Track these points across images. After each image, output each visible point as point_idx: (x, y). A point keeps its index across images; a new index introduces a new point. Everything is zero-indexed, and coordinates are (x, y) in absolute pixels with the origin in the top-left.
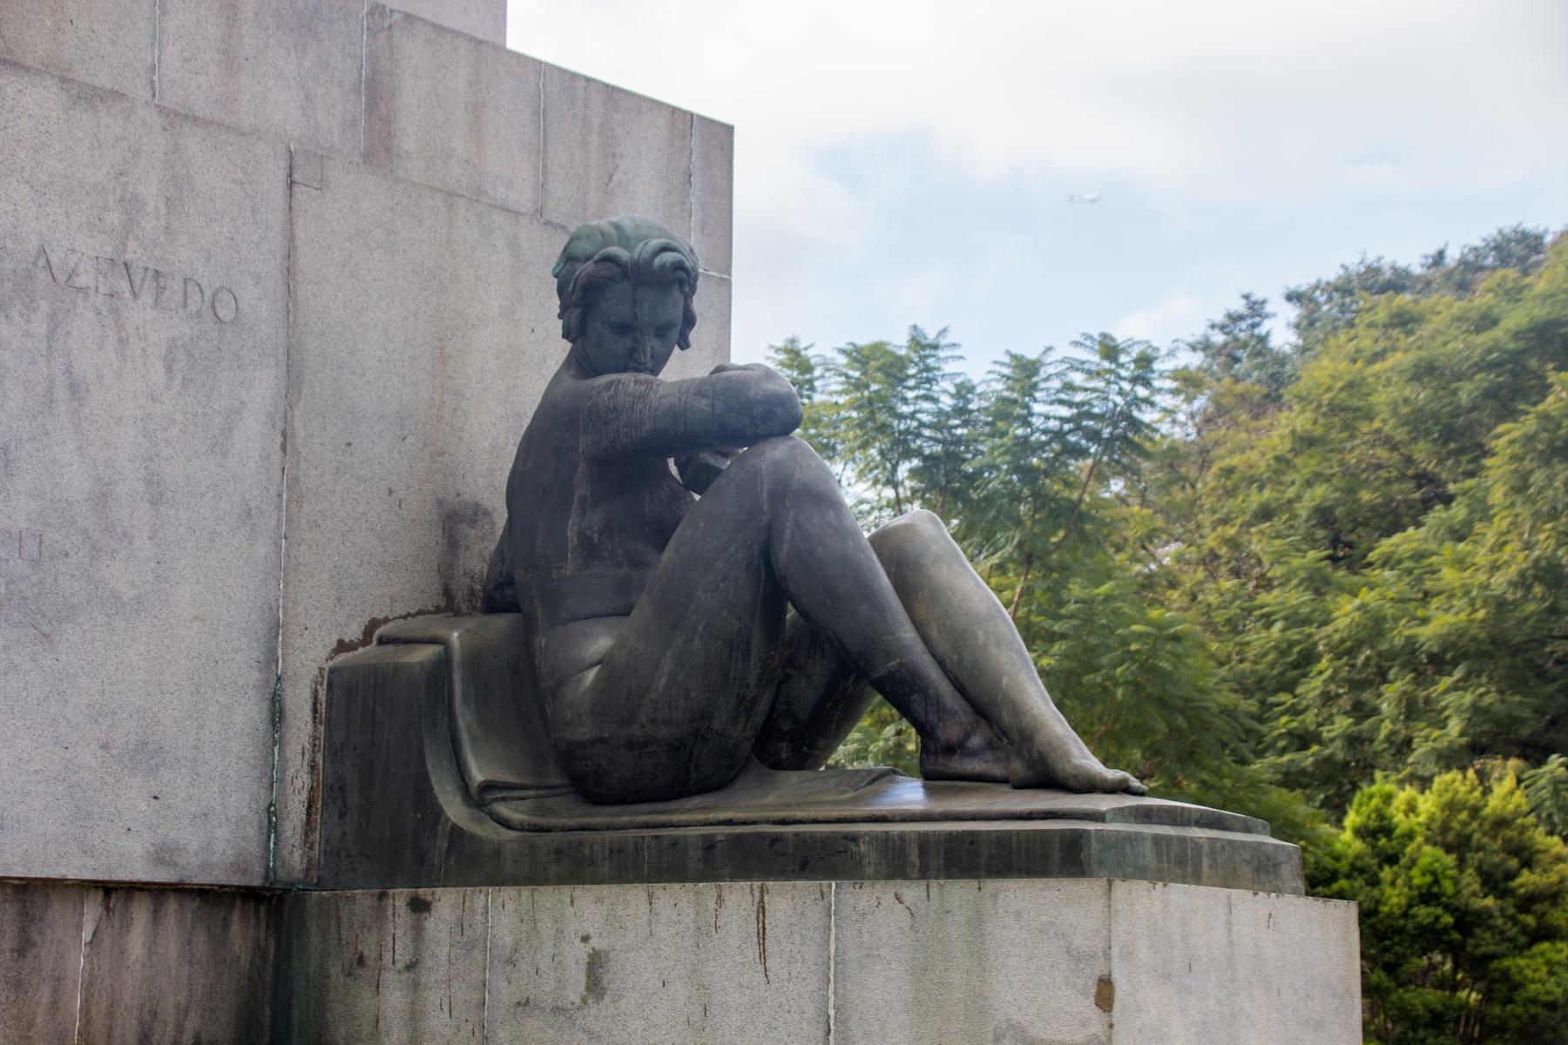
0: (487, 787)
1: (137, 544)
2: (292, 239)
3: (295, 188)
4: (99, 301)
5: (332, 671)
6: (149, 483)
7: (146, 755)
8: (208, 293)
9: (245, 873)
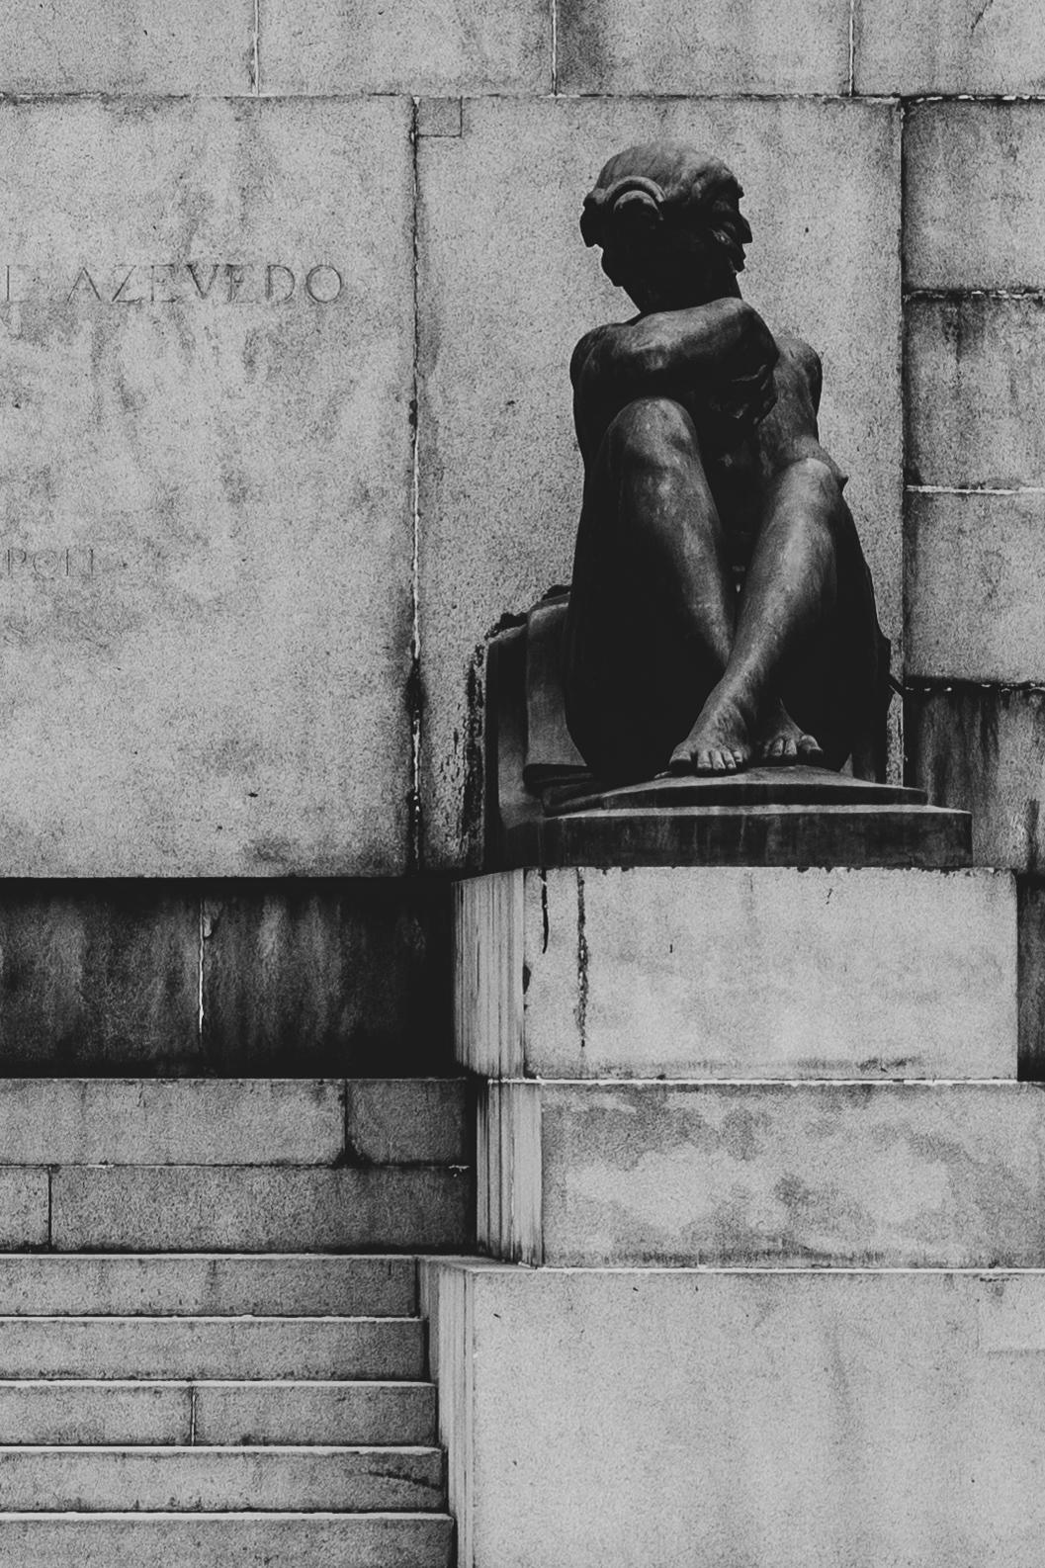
1: (214, 543)
2: (417, 198)
3: (422, 142)
4: (156, 310)
5: (491, 646)
6: (228, 481)
7: (233, 755)
8: (300, 276)
9: (379, 864)
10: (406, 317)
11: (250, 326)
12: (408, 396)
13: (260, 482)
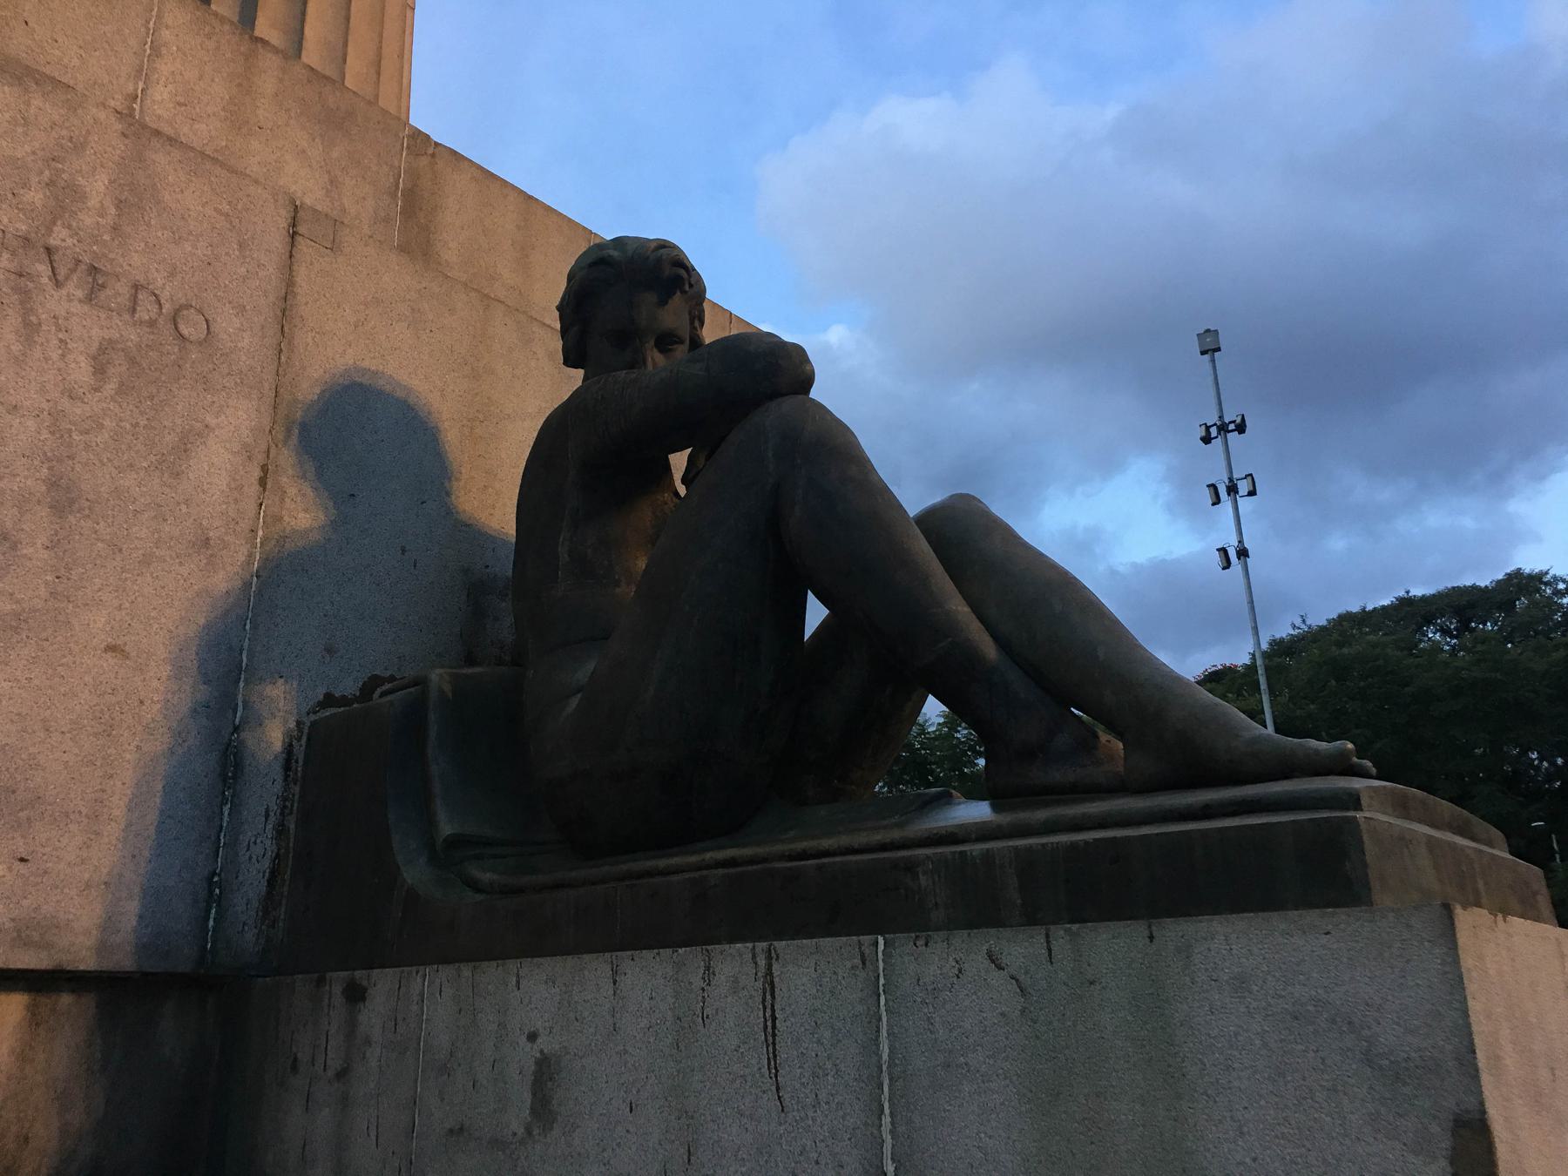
0: (455, 842)
2: (290, 283)
5: (313, 724)
6: (53, 484)
8: (167, 308)
10: (266, 385)
11: (107, 334)
12: (260, 458)
13: (91, 497)
